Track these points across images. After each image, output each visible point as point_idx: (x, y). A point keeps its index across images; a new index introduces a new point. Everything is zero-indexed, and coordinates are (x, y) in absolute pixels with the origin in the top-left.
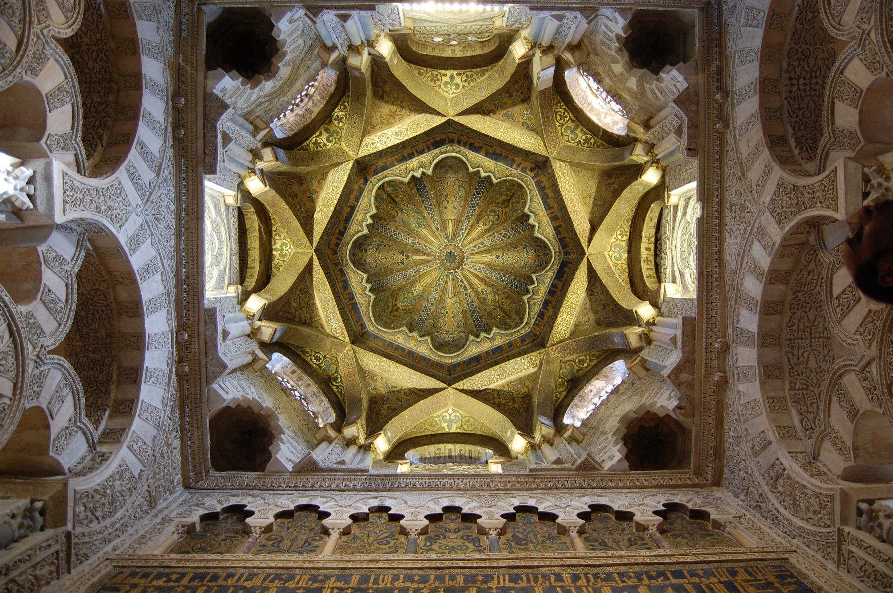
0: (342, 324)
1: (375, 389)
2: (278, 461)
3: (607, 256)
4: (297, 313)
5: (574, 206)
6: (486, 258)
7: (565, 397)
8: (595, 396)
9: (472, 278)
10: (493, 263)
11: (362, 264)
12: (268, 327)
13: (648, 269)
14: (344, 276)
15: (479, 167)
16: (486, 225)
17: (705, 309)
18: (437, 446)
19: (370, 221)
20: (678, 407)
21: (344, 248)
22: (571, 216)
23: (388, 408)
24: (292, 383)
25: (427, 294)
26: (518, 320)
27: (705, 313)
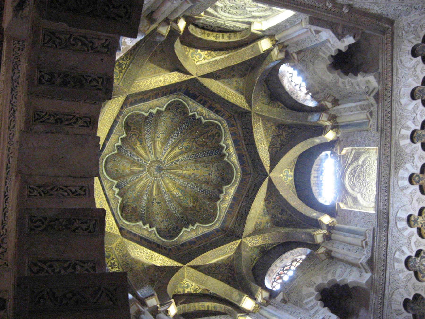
0: (228, 245)
1: (267, 223)
2: (367, 282)
3: (198, 63)
4: (225, 275)
5: (161, 81)
6: (158, 145)
7: (283, 103)
8: (291, 84)
9: (170, 156)
10: (163, 140)
11: (169, 231)
12: (262, 294)
13: (223, 37)
14: (185, 243)
15: (114, 146)
16: (136, 143)
17: (307, 9)
18: (312, 185)
19: (148, 226)
20: (354, 37)
21: (166, 244)
22: (167, 84)
24: (275, 276)
25: (181, 187)
26: (211, 127)
27: (309, 9)
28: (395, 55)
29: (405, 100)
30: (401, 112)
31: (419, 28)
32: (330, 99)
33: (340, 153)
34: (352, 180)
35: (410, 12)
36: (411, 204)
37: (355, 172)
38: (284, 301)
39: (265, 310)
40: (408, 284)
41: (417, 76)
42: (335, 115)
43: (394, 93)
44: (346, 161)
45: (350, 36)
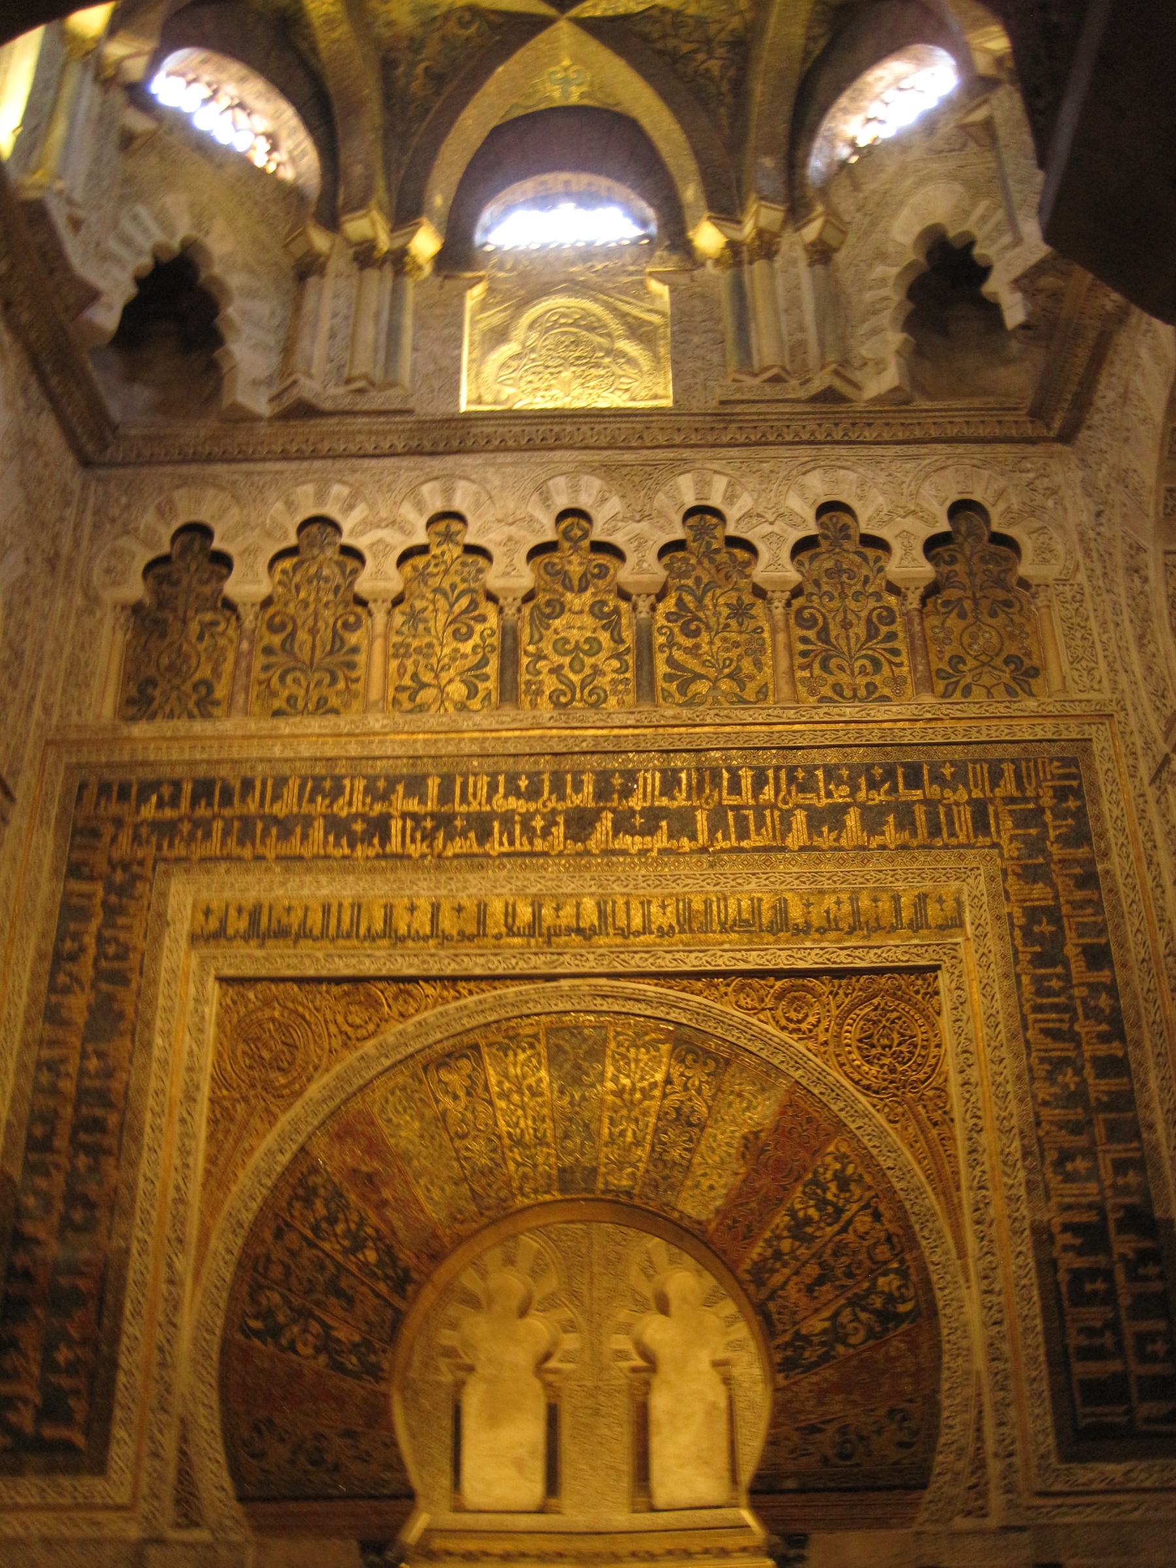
1: (390, 24)
2: (236, 407)
20: (1024, 326)
23: (427, 69)
28: (961, 449)
29: (819, 486)
30: (782, 474)
31: (1040, 524)
32: (832, 238)
33: (651, 274)
34: (562, 321)
35: (1090, 495)
36: (499, 521)
37: (591, 328)
38: (128, 140)
39: (81, 82)
40: (257, 531)
41: (892, 519)
42: (776, 252)
43: (842, 450)
44: (626, 293)
45: (1030, 315)
